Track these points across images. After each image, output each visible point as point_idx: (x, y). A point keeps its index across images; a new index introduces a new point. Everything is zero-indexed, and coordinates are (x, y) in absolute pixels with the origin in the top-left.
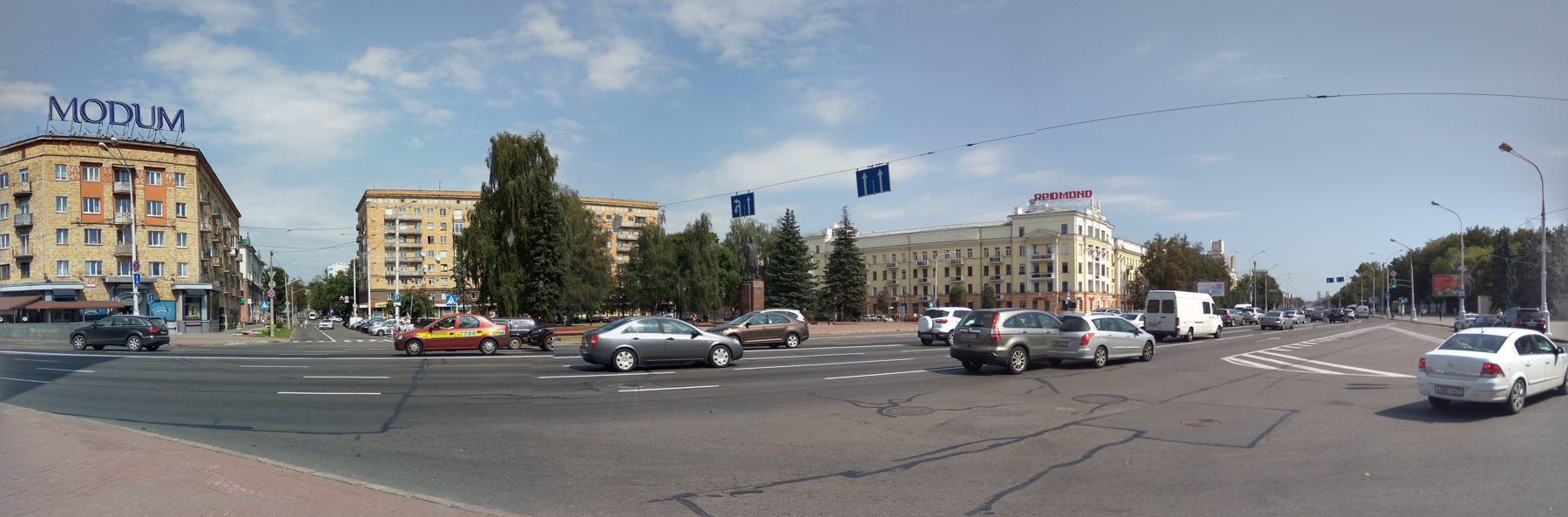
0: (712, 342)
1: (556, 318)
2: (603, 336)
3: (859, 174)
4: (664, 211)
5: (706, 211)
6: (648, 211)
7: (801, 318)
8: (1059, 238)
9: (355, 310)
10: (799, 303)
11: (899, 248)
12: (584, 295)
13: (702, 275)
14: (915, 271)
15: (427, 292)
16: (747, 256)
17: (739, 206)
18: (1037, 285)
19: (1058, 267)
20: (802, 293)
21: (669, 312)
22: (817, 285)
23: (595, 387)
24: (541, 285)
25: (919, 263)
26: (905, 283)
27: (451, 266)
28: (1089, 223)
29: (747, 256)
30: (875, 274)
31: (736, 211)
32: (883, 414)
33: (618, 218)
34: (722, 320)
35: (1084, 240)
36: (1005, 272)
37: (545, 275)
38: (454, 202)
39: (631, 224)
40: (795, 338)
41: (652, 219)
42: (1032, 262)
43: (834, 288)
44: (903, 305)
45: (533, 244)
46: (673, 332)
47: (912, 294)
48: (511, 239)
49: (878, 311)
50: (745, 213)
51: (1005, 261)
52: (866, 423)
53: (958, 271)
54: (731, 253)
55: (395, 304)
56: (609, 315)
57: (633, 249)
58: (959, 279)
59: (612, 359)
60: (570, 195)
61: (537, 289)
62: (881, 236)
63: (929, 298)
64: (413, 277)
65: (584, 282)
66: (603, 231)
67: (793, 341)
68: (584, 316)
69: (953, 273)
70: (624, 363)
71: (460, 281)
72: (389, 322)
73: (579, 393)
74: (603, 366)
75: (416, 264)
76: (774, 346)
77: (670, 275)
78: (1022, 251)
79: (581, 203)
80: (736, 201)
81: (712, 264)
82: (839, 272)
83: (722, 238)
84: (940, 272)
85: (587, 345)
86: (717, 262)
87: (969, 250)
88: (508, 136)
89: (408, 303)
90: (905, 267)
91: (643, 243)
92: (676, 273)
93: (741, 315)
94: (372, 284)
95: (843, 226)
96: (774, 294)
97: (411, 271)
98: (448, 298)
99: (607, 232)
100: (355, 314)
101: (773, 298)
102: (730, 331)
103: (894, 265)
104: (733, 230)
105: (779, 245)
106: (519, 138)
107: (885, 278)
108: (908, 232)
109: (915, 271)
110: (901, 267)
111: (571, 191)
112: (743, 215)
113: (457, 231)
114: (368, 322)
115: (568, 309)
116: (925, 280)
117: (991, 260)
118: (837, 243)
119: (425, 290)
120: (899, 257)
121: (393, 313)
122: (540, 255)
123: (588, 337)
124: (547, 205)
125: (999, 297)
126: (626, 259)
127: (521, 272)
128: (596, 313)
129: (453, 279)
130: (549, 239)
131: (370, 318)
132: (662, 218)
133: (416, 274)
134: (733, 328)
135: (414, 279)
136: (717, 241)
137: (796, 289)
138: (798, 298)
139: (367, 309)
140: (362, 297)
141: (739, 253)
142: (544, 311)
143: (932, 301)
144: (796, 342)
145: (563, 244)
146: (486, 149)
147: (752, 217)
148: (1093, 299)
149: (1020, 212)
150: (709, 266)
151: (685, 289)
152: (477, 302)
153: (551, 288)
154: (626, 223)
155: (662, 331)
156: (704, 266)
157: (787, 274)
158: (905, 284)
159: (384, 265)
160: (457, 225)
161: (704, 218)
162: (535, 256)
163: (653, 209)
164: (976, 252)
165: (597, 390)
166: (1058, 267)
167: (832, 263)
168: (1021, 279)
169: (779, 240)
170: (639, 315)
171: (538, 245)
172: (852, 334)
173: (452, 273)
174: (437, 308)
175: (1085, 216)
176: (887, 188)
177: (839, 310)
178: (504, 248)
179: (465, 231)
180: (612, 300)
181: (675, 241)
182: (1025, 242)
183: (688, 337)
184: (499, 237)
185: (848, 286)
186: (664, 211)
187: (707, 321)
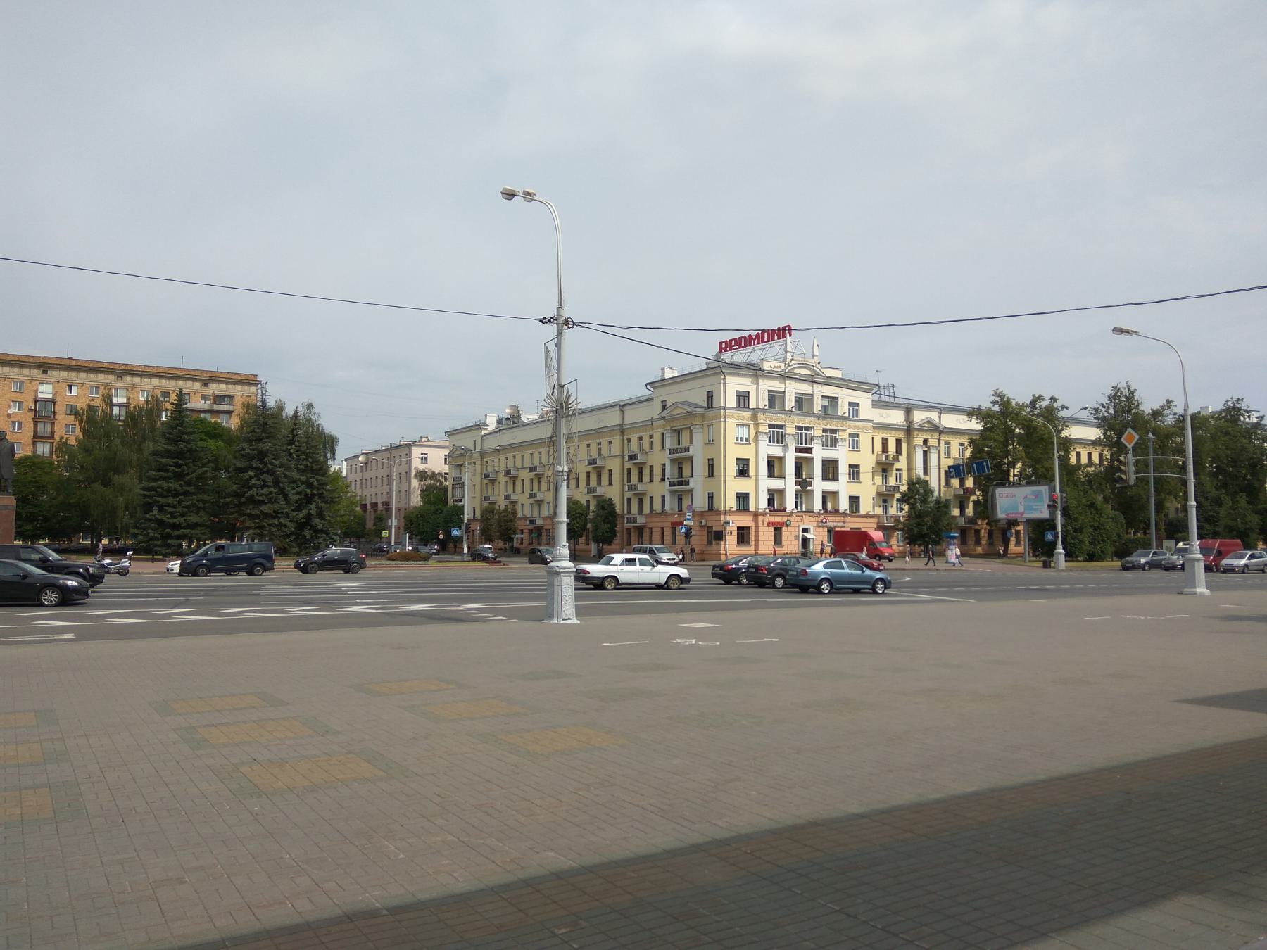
19: (700, 467)
28: (768, 385)
35: (754, 417)
148: (783, 524)
175: (754, 370)
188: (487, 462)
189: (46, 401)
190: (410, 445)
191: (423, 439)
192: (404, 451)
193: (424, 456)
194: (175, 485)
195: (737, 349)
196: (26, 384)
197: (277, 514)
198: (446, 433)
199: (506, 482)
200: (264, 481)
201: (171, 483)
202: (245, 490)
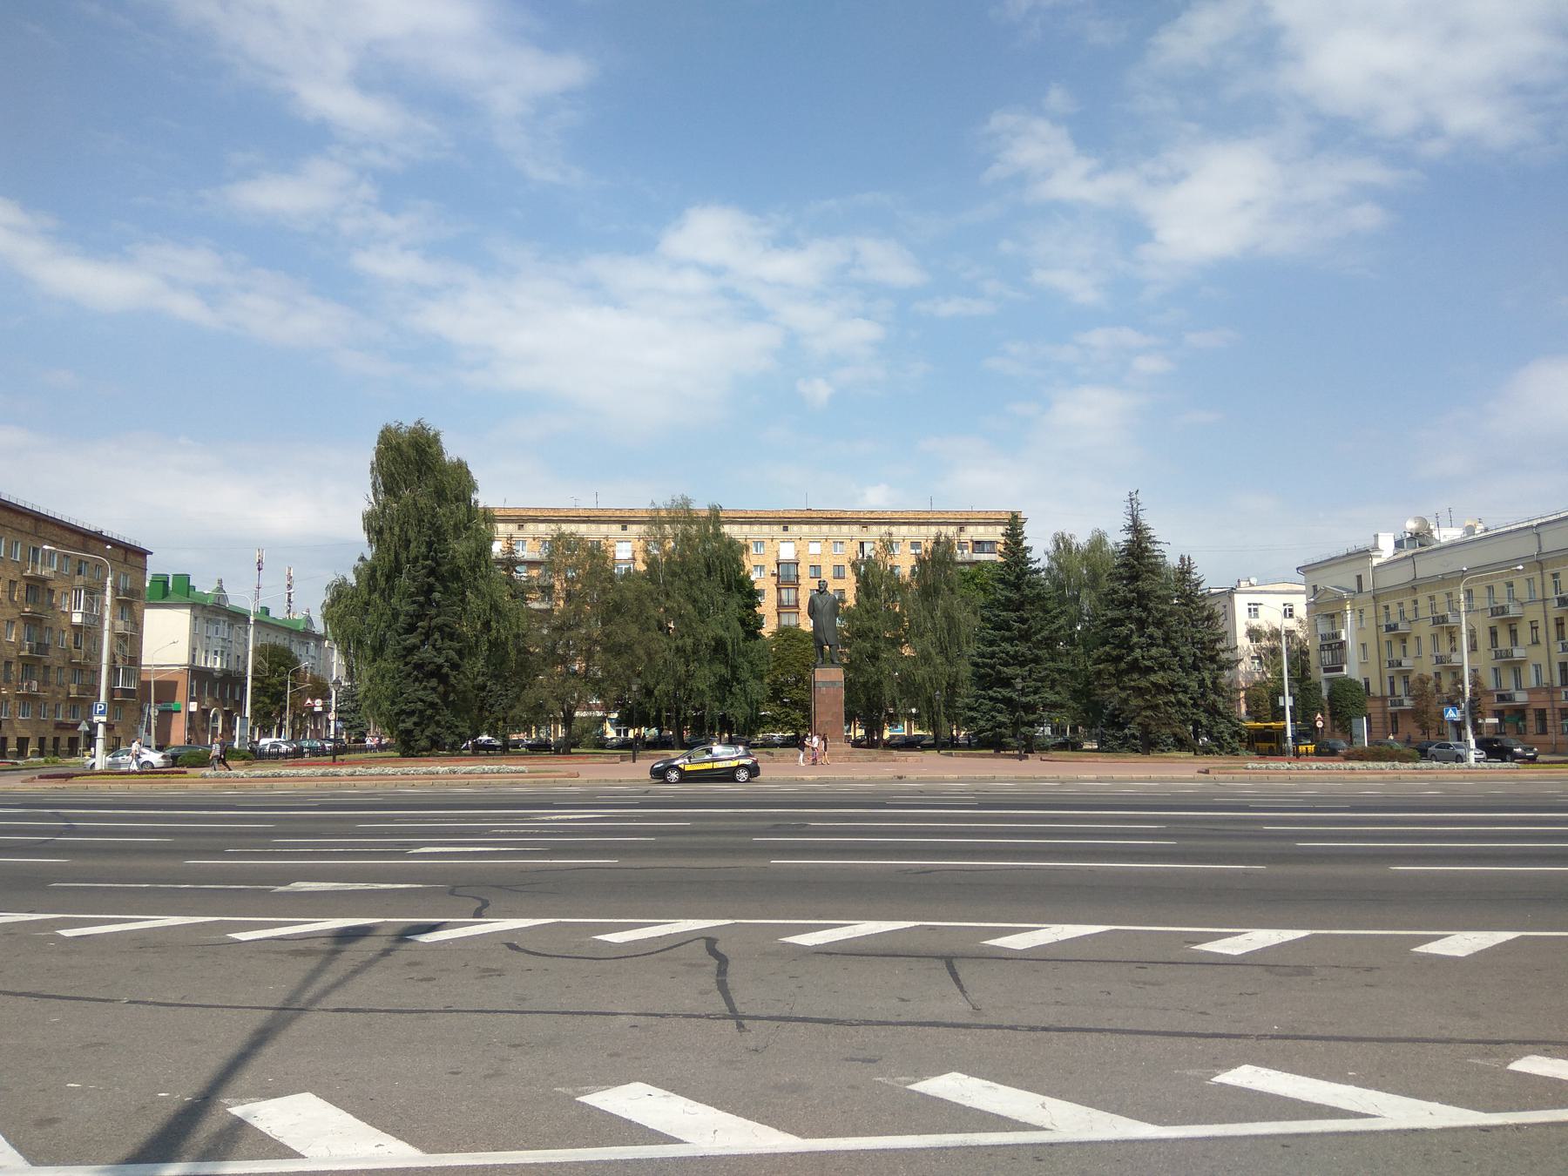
108: (1535, 523)
188: (1387, 607)
189: (788, 563)
190: (1232, 591)
191: (1242, 584)
192: (1224, 600)
193: (1252, 607)
194: (1022, 648)
196: (768, 543)
197: (1171, 688)
198: (1298, 569)
199: (1389, 643)
200: (1151, 637)
201: (1017, 645)
202: (1124, 651)
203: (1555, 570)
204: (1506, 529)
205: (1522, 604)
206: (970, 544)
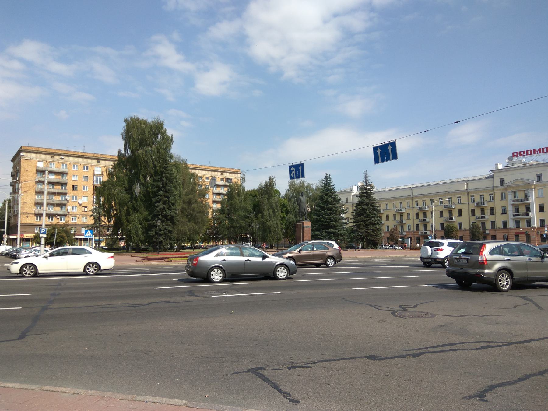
0: (276, 262)
1: (169, 246)
2: (202, 258)
3: (375, 149)
4: (244, 175)
5: (272, 175)
6: (234, 175)
7: (336, 246)
8: (534, 185)
9: (5, 240)
10: (335, 236)
11: (405, 198)
12: (189, 230)
13: (270, 217)
14: (417, 214)
15: (69, 227)
16: (299, 205)
17: (294, 172)
18: (518, 223)
19: (535, 208)
20: (337, 229)
21: (247, 242)
22: (347, 224)
23: (195, 294)
24: (159, 223)
25: (420, 208)
26: (410, 222)
27: (90, 207)
29: (299, 205)
30: (388, 216)
31: (292, 175)
32: (395, 316)
33: (214, 179)
34: (283, 248)
36: (489, 213)
37: (163, 216)
38: (95, 162)
39: (222, 183)
40: (332, 260)
41: (236, 180)
42: (513, 205)
43: (359, 226)
44: (408, 238)
45: (155, 195)
46: (251, 255)
47: (416, 230)
48: (138, 190)
49: (390, 242)
50: (298, 177)
51: (489, 205)
52: (384, 321)
53: (451, 213)
54: (288, 203)
55: (41, 236)
56: (207, 244)
57: (223, 200)
58: (452, 219)
59: (208, 274)
60: (181, 162)
61: (156, 226)
62: (392, 190)
63: (428, 233)
64: (58, 215)
65: (189, 221)
66: (203, 187)
67: (331, 262)
68: (189, 245)
69: (446, 215)
70: (216, 277)
71: (97, 219)
72: (35, 250)
73: (184, 299)
74: (201, 279)
75: (61, 205)
76: (318, 265)
77: (248, 217)
78: (503, 197)
79: (189, 168)
80: (292, 169)
81: (276, 210)
82: (362, 215)
83: (283, 193)
84: (436, 214)
85: (190, 265)
86: (279, 209)
87: (458, 197)
88: (138, 119)
89: (52, 235)
90: (410, 211)
91: (229, 196)
92: (252, 216)
93: (296, 244)
94: (22, 219)
95: (365, 184)
96: (317, 230)
97: (57, 210)
98: (86, 232)
99: (206, 188)
100: (5, 243)
101: (317, 233)
102: (288, 255)
103: (401, 210)
104: (290, 188)
105: (321, 198)
106: (146, 121)
107: (395, 219)
108: (411, 186)
109: (417, 214)
110: (406, 211)
111: (182, 160)
112: (296, 178)
113: (97, 182)
114: (17, 250)
115: (178, 240)
116: (425, 220)
117: (477, 204)
118: (361, 195)
119: (68, 225)
120: (405, 204)
121: (39, 243)
122: (159, 202)
123: (191, 259)
124: (165, 168)
125: (485, 232)
126: (219, 206)
127: (145, 213)
128: (198, 243)
129: (92, 218)
130: (166, 191)
131: (18, 246)
132: (243, 179)
133: (61, 213)
134: (290, 253)
135: (59, 217)
136: (279, 195)
137: (333, 227)
138: (334, 233)
139: (16, 239)
140: (12, 229)
141: (294, 203)
142: (161, 242)
143: (431, 235)
144: (333, 263)
145: (175, 195)
146: (122, 127)
147: (303, 179)
149: (500, 167)
150: (274, 212)
151: (258, 227)
152: (110, 235)
153: (167, 225)
154: (219, 182)
155: (242, 255)
156: (271, 212)
157: (327, 217)
158: (410, 223)
159: (33, 205)
160: (97, 178)
161: (271, 181)
162: (156, 203)
163: (237, 173)
164: (464, 199)
165: (197, 296)
166: (535, 208)
167: (357, 209)
168: (504, 218)
169: (320, 194)
170: (227, 244)
171: (158, 195)
172: (372, 258)
173: (91, 213)
174: (77, 239)
176: (395, 157)
177: (363, 241)
178: (133, 197)
179: (103, 183)
180: (208, 234)
181: (251, 195)
182: (506, 189)
183: (260, 259)
184: (130, 190)
185: (369, 225)
186: (244, 175)
187: (272, 248)
195: (525, 155)
203: (417, 200)
204: (396, 188)
205: (405, 208)
206: (225, 179)
